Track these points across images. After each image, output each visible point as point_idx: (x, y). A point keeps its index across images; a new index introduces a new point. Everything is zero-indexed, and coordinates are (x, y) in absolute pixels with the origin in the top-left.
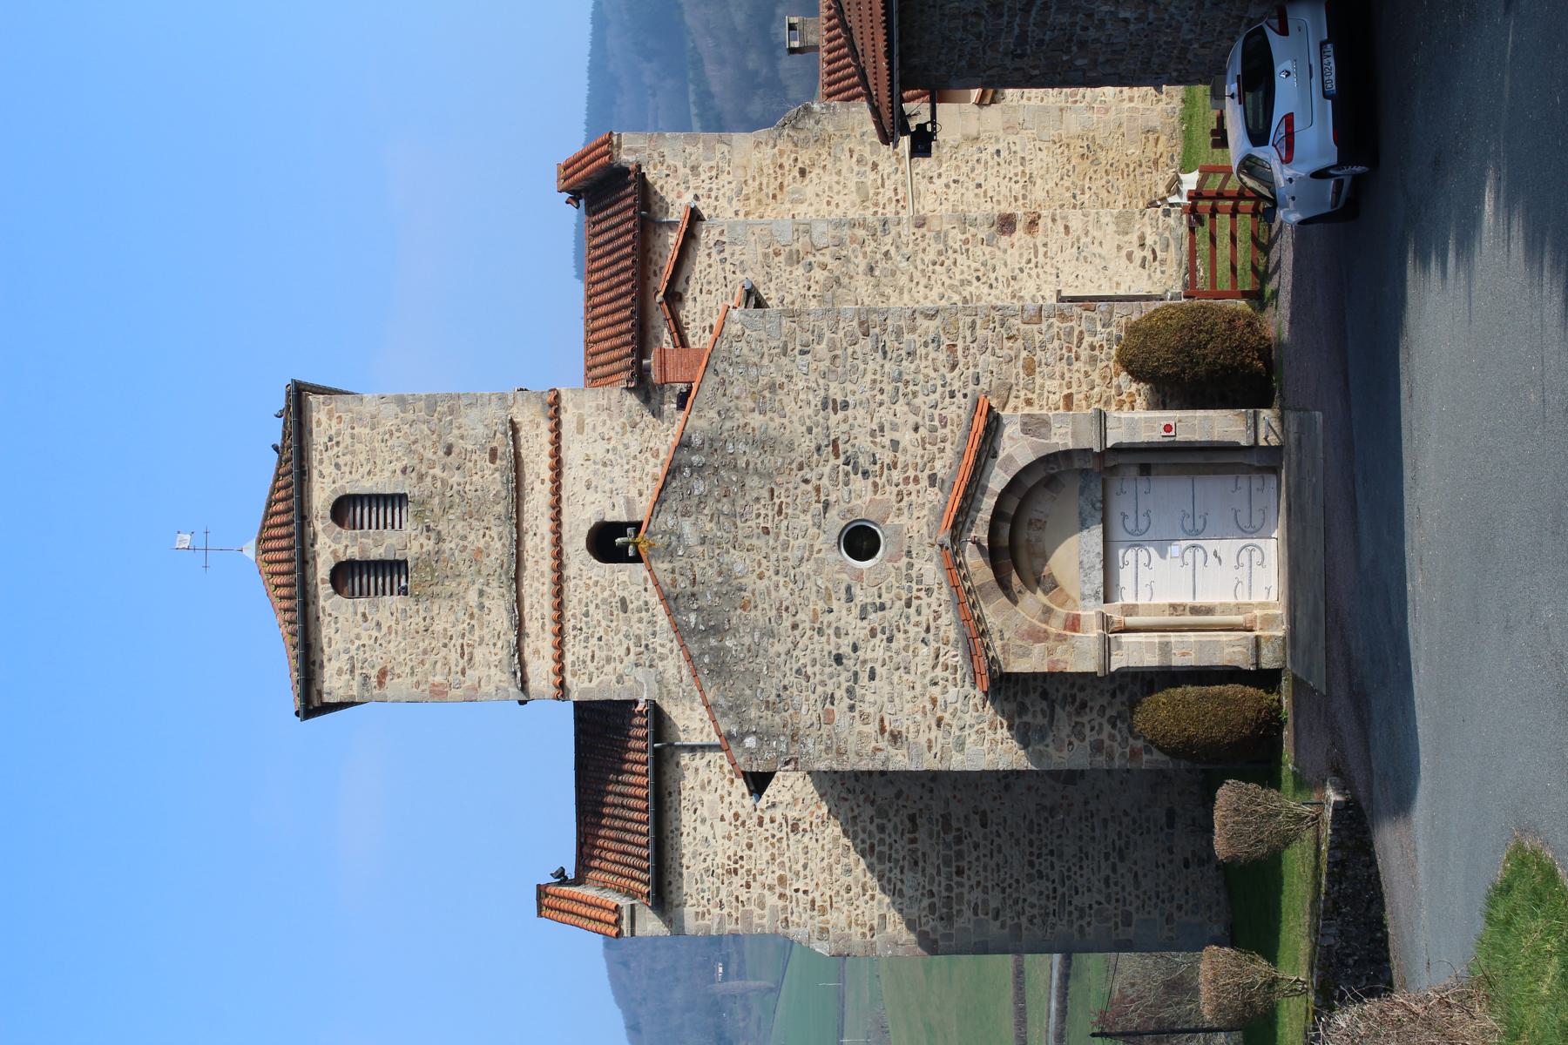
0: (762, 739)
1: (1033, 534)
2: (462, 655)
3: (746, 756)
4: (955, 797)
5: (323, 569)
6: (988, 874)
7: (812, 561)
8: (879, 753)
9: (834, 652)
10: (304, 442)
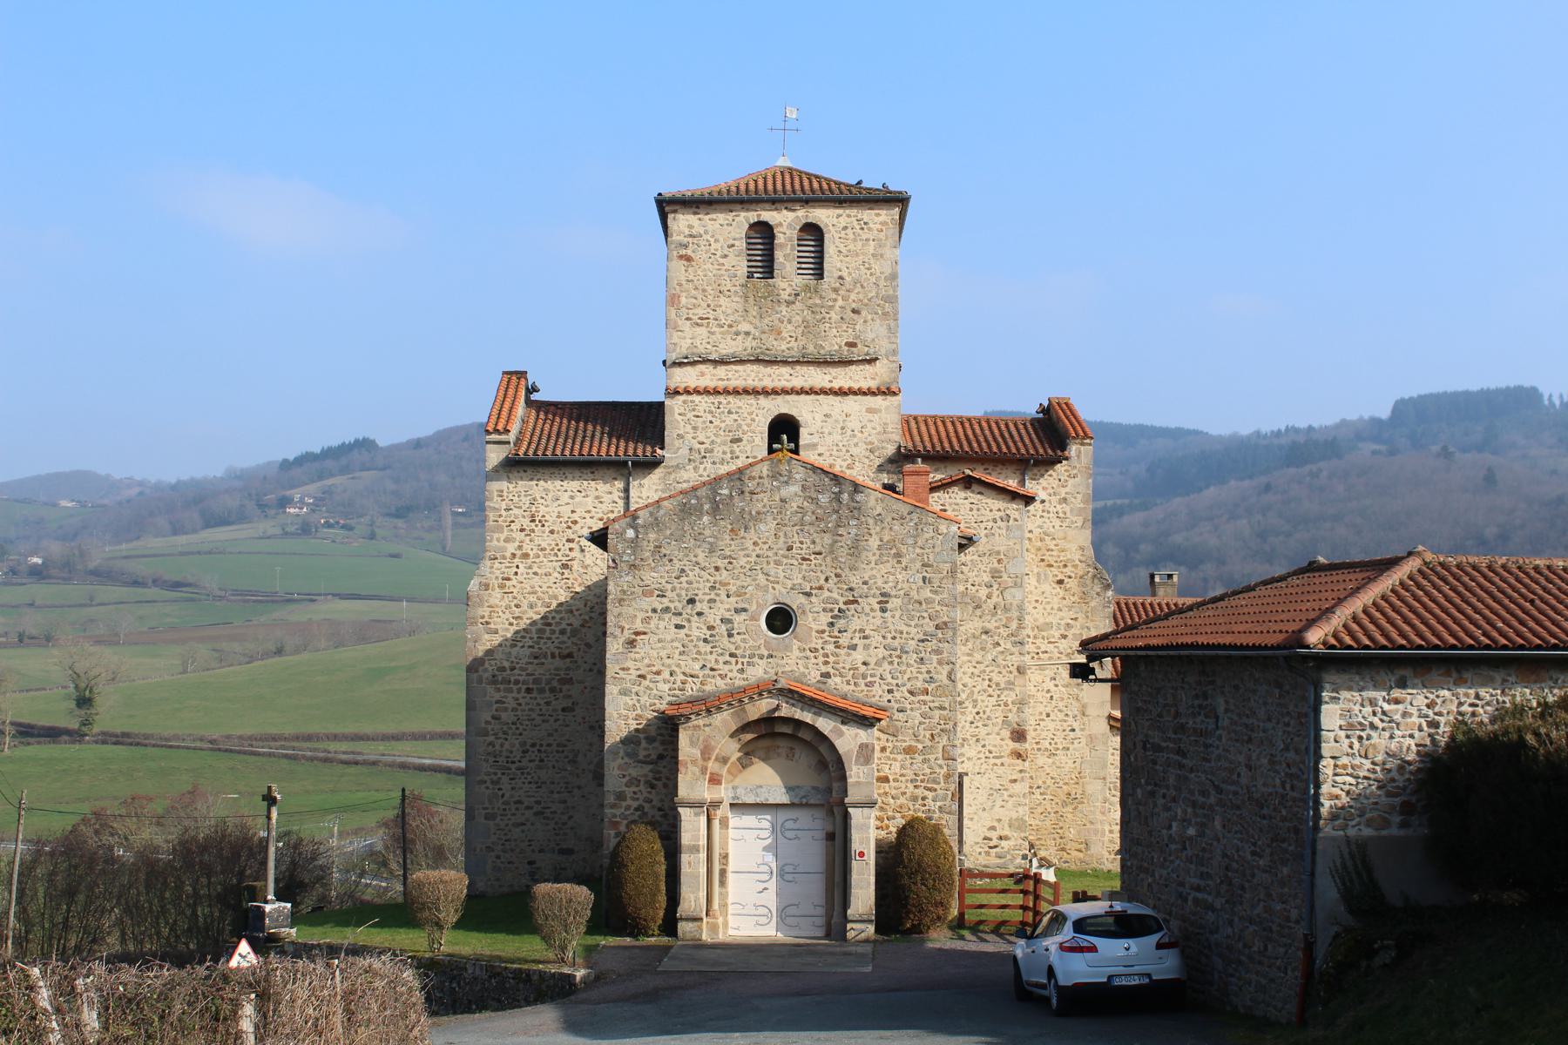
6: (526, 713)
7: (766, 582)
8: (620, 630)
9: (697, 598)
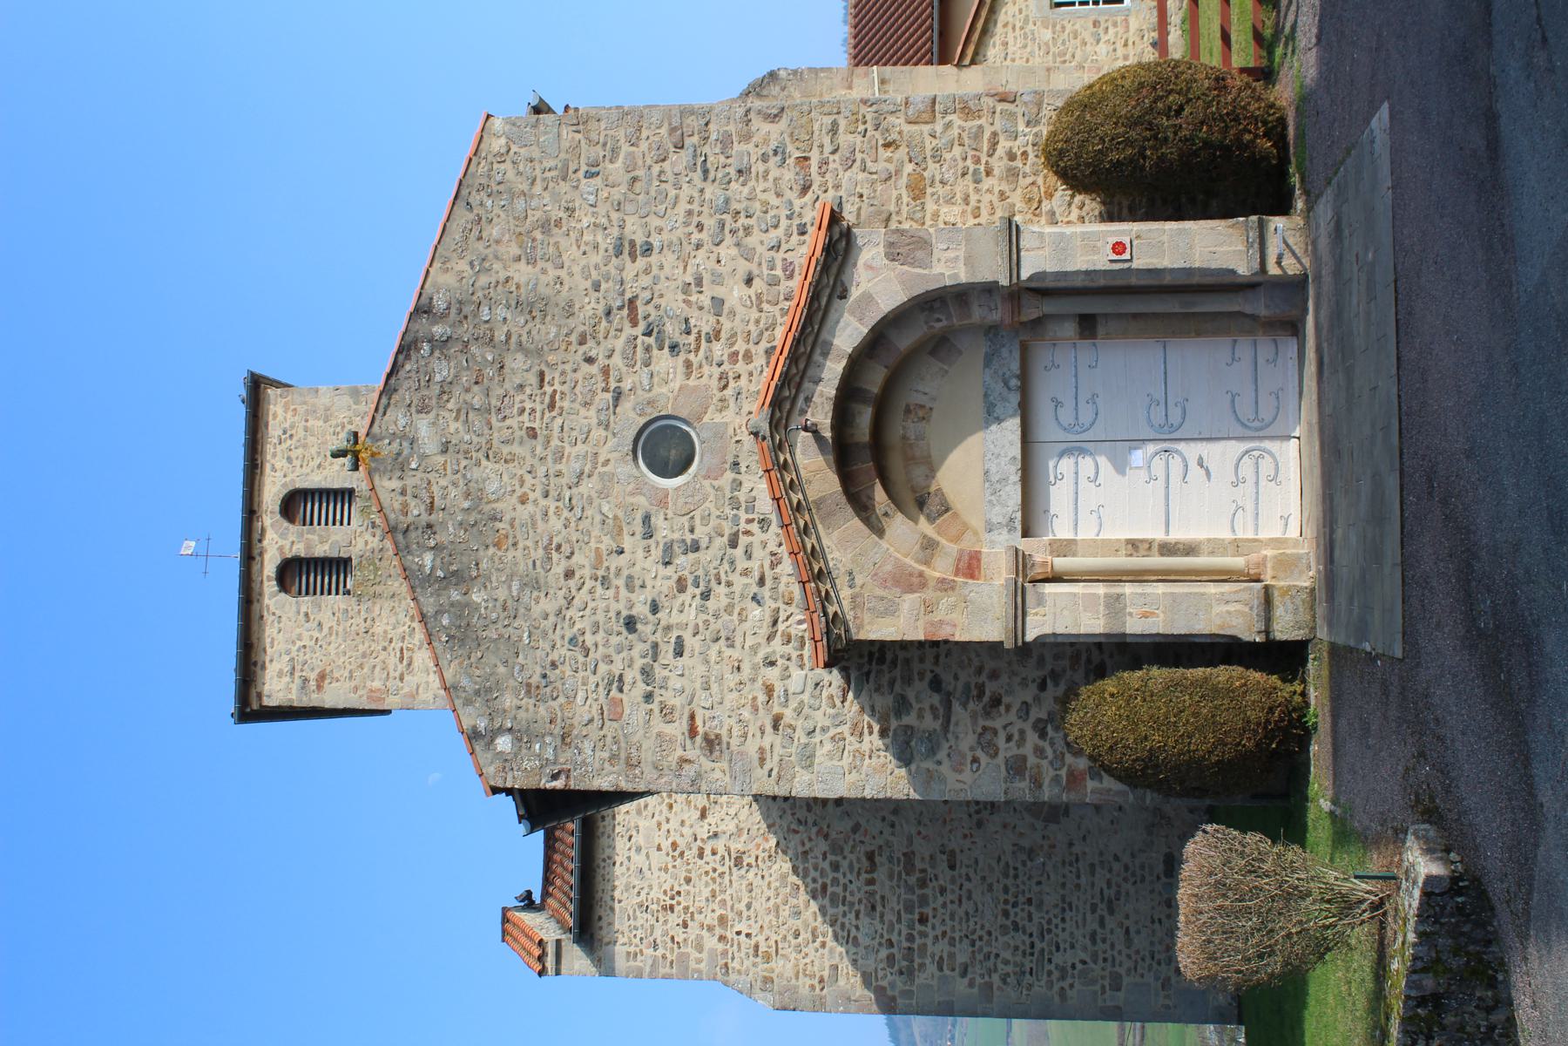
2: (402, 659)
3: (498, 763)
4: (919, 833)
5: (269, 566)
6: (956, 924)
7: (595, 477)
8: (686, 766)
9: (625, 613)
10: (259, 436)
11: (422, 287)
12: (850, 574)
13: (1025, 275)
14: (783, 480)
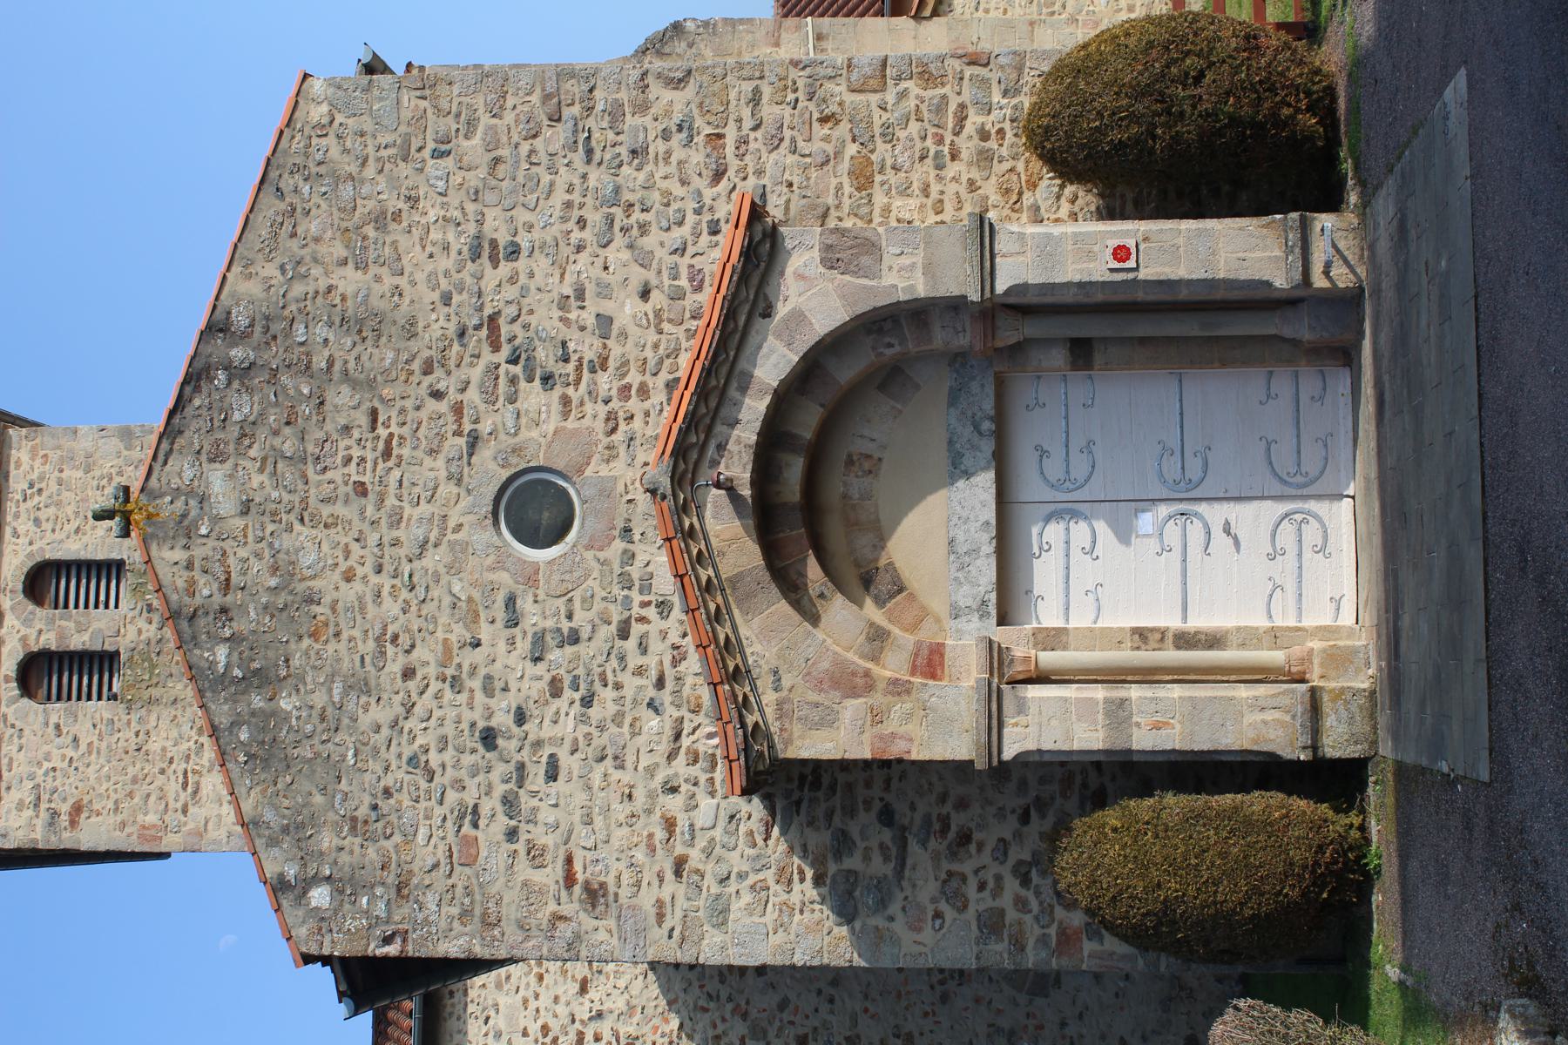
0: (342, 892)
1: (856, 485)
2: (185, 785)
3: (312, 923)
4: (866, 1010)
7: (444, 547)
8: (561, 925)
9: (481, 724)
11: (217, 298)
12: (776, 673)
13: (1001, 287)
14: (689, 552)
